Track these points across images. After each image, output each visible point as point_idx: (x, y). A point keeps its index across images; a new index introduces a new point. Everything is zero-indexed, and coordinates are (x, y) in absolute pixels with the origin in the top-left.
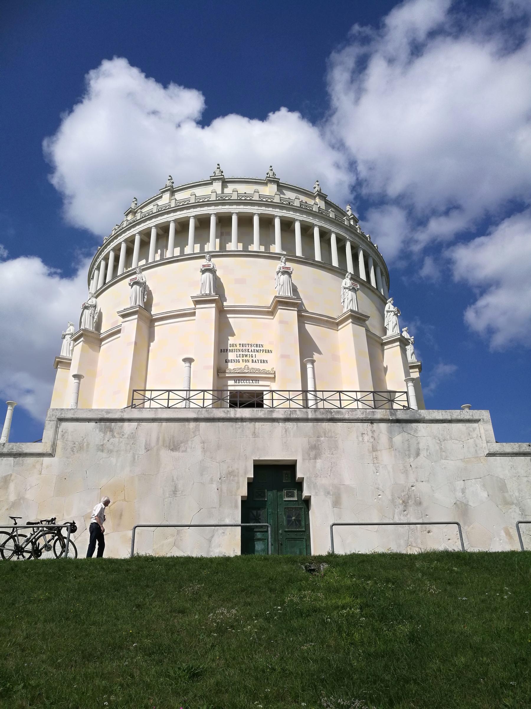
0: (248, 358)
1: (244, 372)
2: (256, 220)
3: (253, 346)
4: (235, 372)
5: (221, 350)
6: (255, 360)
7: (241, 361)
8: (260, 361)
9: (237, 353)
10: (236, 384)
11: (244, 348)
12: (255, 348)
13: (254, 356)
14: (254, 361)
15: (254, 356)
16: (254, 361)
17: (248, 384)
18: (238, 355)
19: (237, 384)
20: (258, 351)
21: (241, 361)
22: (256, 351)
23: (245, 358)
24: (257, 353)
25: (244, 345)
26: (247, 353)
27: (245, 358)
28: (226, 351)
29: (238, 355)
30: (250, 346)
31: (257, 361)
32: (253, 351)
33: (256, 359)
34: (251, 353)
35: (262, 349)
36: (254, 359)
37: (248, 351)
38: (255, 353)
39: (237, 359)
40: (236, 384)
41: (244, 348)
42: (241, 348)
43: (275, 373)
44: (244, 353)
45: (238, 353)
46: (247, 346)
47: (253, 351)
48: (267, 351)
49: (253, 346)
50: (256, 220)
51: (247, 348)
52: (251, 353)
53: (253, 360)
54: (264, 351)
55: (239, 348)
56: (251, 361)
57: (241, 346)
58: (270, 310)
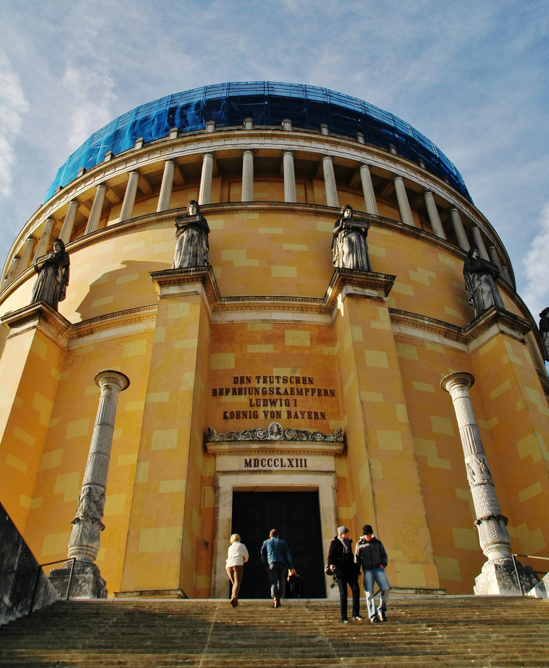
0: (278, 408)
1: (268, 438)
2: (288, 161)
3: (289, 380)
4: (248, 439)
5: (215, 391)
6: (296, 412)
7: (262, 415)
8: (306, 415)
9: (251, 397)
10: (249, 468)
11: (268, 386)
12: (294, 386)
13: (292, 403)
14: (293, 414)
15: (292, 403)
16: (293, 414)
17: (279, 468)
18: (254, 401)
19: (253, 468)
20: (300, 393)
21: (262, 415)
22: (295, 391)
23: (269, 408)
24: (299, 398)
25: (268, 380)
26: (275, 396)
27: (269, 408)
28: (224, 392)
29: (254, 401)
30: (281, 380)
31: (300, 415)
32: (289, 392)
33: (298, 409)
34: (286, 397)
35: (309, 386)
36: (293, 410)
37: (278, 393)
38: (295, 397)
39: (253, 409)
40: (249, 468)
41: (268, 386)
42: (261, 385)
43: (345, 442)
44: (267, 397)
45: (254, 398)
46: (275, 381)
47: (289, 392)
48: (323, 392)
49: (289, 380)
50: (288, 161)
51: (275, 385)
52: (284, 398)
53: (289, 413)
54: (316, 393)
55: (257, 386)
56: (284, 415)
57: (261, 380)
58: (324, 305)
